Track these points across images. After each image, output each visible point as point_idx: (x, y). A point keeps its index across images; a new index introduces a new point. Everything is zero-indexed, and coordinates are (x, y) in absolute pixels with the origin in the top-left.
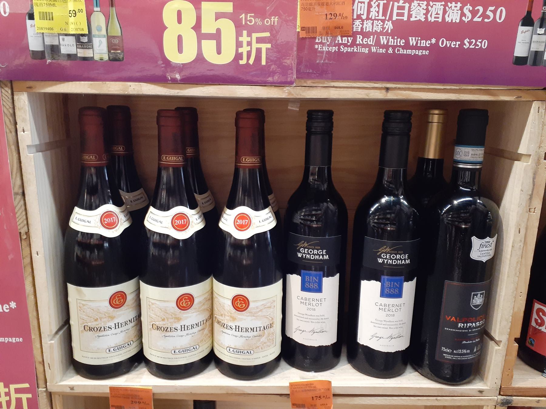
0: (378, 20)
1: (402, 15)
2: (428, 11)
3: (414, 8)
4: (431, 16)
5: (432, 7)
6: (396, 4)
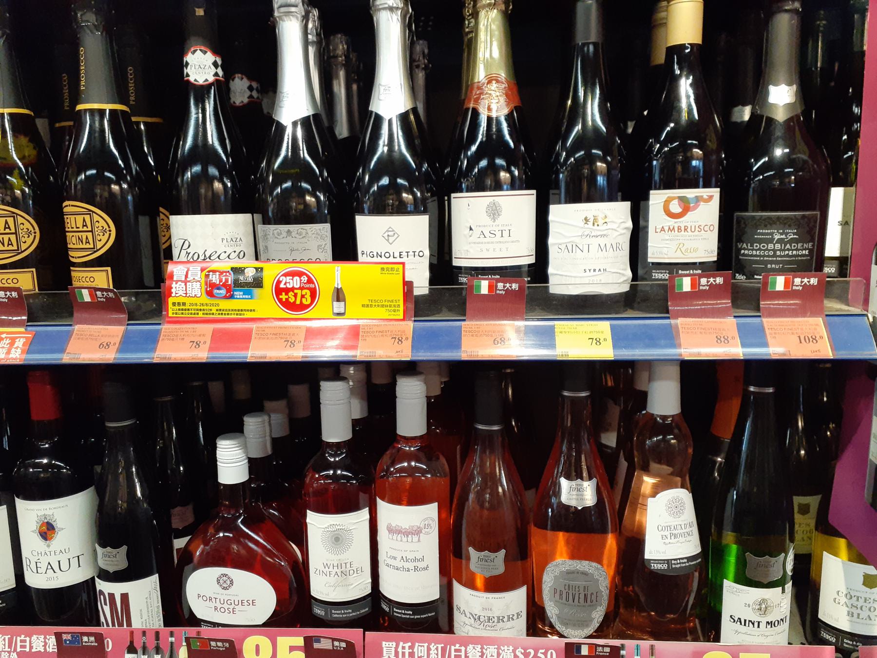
0: (5, 652)
1: (25, 647)
2: (46, 644)
3: (34, 641)
4: (49, 647)
5: (49, 640)
6: (19, 639)
